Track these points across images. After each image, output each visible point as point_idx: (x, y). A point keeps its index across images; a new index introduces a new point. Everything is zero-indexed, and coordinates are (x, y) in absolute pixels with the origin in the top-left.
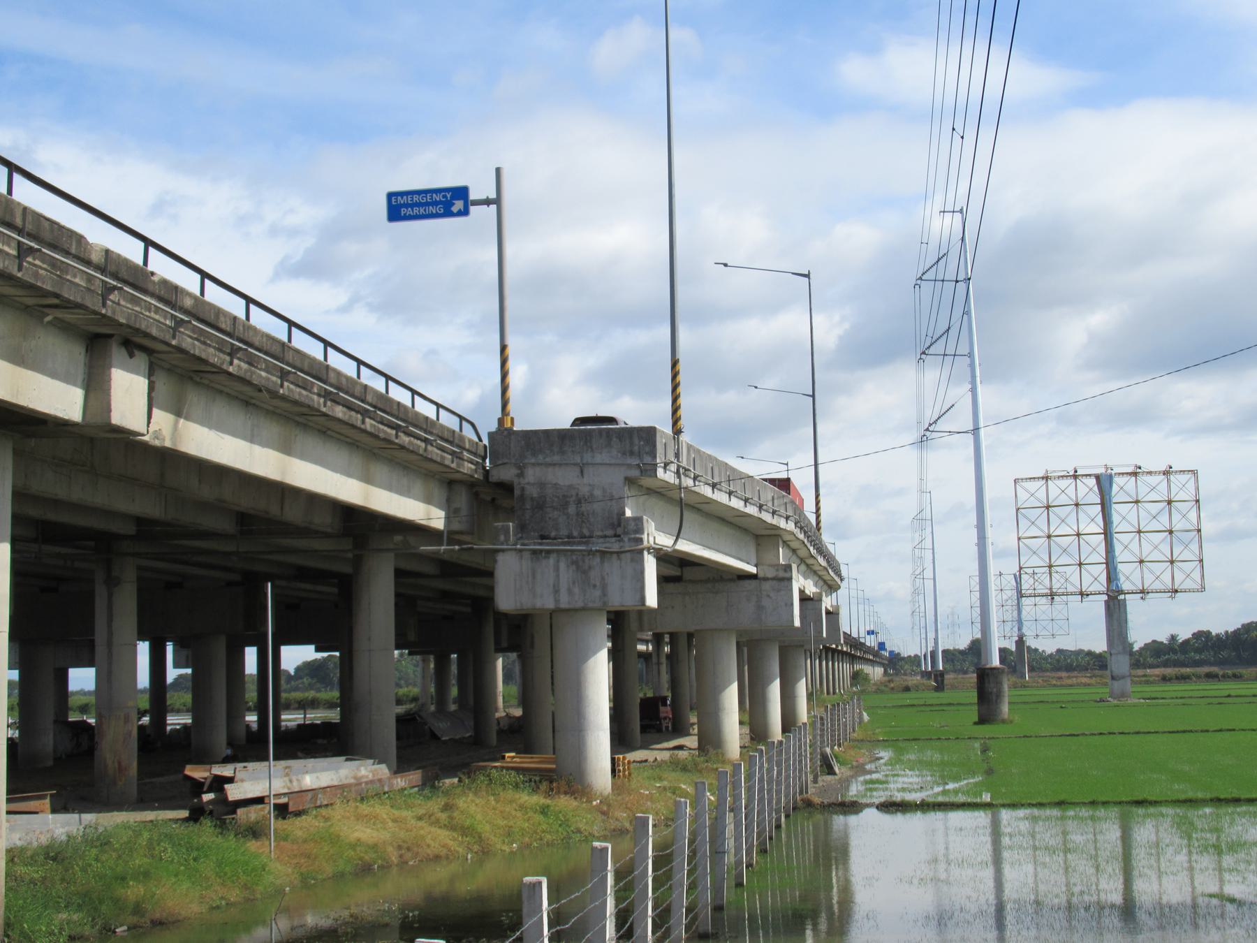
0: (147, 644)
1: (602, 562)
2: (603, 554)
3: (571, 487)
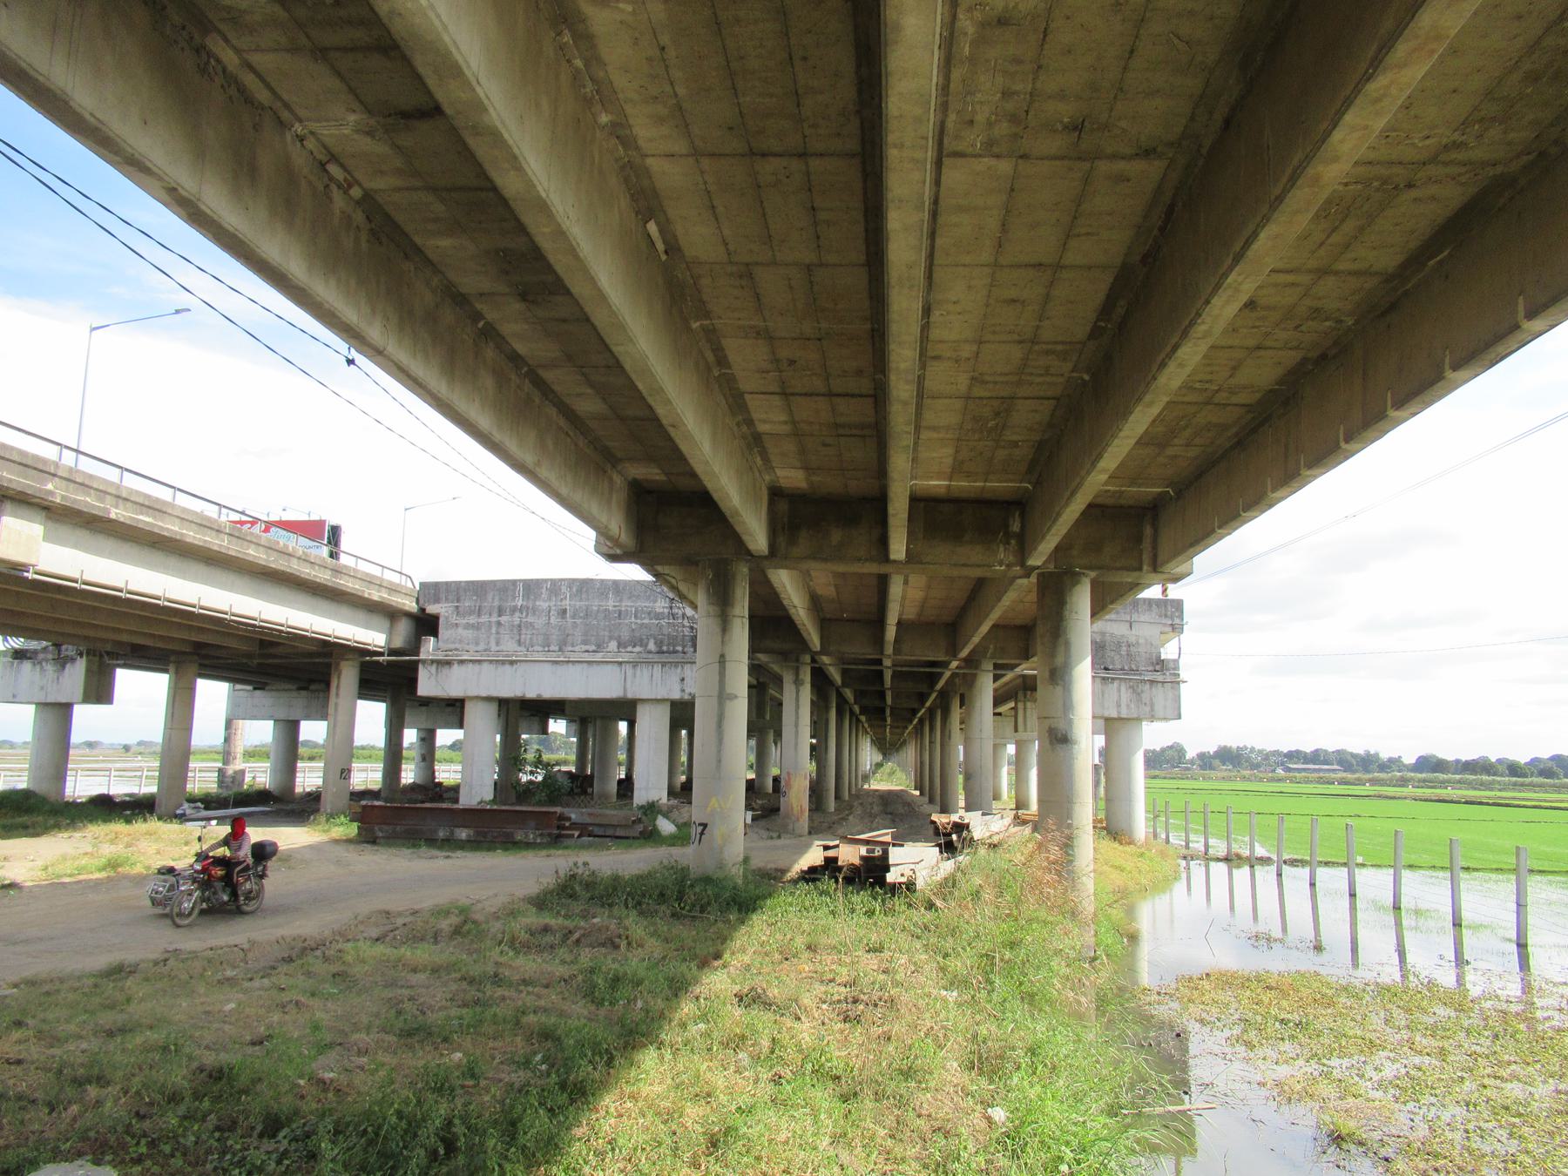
0: (551, 721)
1: (1151, 688)
2: (1152, 682)
3: (1123, 636)
